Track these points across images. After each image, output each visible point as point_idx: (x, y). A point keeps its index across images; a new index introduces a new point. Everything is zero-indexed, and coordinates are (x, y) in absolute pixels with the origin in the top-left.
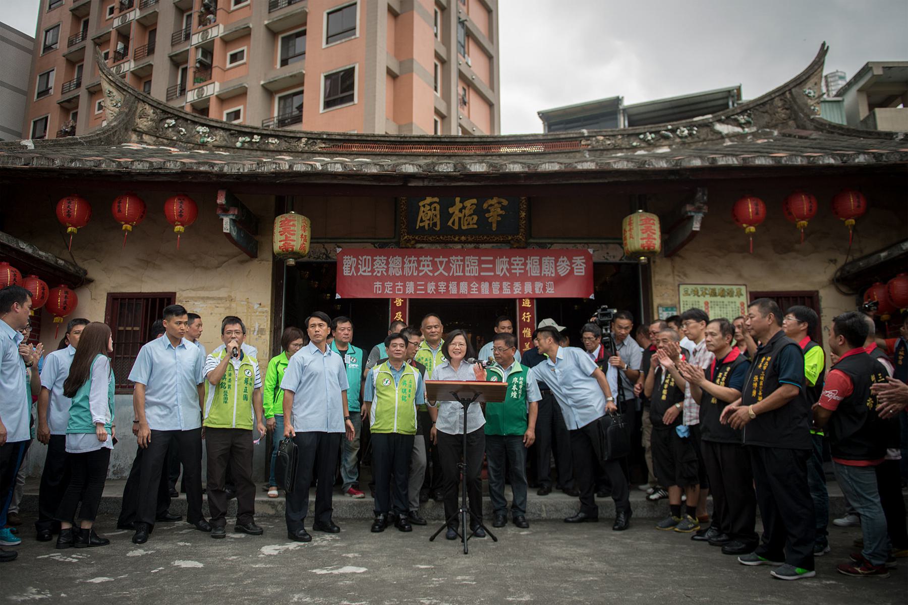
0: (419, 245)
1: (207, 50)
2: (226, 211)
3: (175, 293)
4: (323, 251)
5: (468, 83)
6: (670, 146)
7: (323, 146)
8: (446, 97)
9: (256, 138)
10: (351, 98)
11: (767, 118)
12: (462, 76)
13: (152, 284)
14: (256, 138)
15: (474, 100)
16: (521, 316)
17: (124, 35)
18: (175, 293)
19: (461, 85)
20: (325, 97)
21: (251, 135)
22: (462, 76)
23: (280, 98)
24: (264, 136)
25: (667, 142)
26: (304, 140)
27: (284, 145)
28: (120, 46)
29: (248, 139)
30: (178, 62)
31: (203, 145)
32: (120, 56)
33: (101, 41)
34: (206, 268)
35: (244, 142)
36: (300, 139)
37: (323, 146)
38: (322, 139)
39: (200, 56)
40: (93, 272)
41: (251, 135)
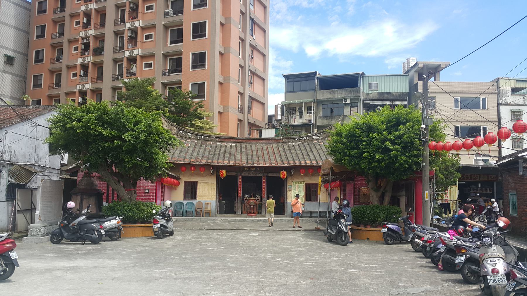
1: (134, 31)
5: (253, 48)
8: (244, 58)
9: (203, 137)
10: (204, 66)
11: (325, 135)
12: (251, 45)
13: (193, 179)
14: (203, 137)
15: (256, 55)
17: (87, 14)
19: (251, 49)
20: (192, 64)
21: (201, 136)
22: (251, 45)
23: (170, 59)
27: (209, 139)
28: (85, 20)
30: (118, 34)
31: (189, 138)
32: (86, 26)
33: (73, 16)
39: (130, 34)
41: (201, 136)
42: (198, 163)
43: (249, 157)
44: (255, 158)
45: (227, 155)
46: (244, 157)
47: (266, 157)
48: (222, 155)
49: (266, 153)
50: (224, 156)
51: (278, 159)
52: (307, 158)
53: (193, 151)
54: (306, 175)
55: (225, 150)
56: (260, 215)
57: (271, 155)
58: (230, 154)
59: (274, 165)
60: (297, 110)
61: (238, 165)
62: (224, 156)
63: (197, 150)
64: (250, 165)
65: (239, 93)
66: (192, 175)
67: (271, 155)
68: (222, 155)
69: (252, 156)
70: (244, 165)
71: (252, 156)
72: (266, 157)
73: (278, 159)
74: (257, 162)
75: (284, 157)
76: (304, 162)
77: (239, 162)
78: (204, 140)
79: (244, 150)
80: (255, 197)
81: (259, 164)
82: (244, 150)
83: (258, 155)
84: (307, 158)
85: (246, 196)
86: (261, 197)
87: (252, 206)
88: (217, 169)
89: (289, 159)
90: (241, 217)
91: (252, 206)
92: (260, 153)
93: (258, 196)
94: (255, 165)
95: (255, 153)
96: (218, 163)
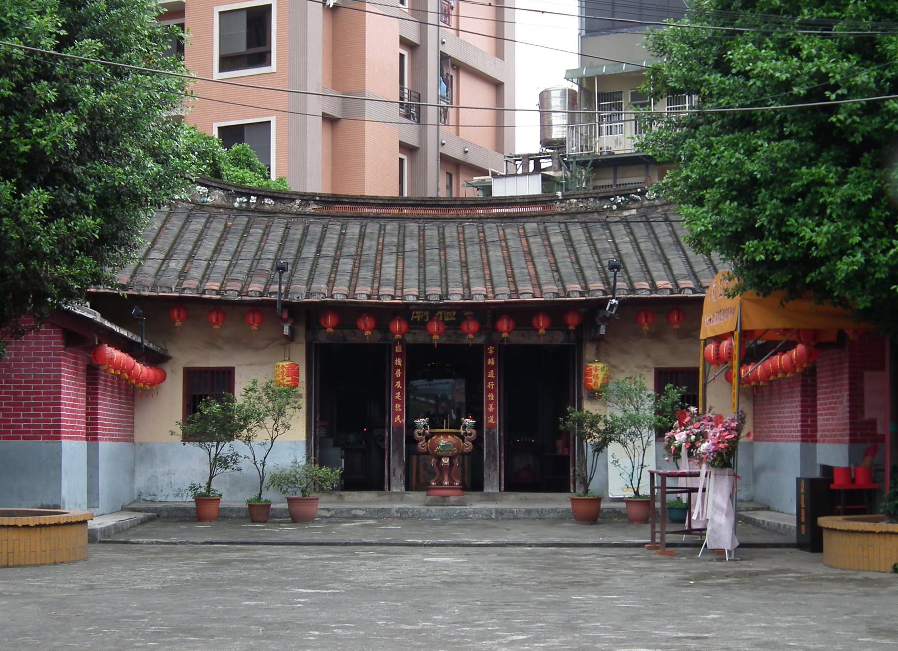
0: (412, 331)
2: (286, 321)
3: (234, 368)
4: (341, 335)
6: (637, 209)
7: (316, 207)
9: (253, 199)
13: (215, 361)
14: (253, 199)
16: (487, 385)
18: (234, 368)
21: (248, 196)
24: (260, 198)
25: (636, 205)
26: (298, 202)
29: (246, 200)
34: (257, 349)
35: (241, 203)
36: (294, 200)
37: (316, 207)
38: (315, 201)
40: (172, 352)
41: (248, 196)
42: (232, 296)
43: (433, 269)
44: (454, 274)
45: (346, 265)
46: (412, 273)
47: (499, 269)
48: (325, 265)
49: (496, 254)
50: (335, 266)
51: (545, 275)
52: (657, 269)
53: (217, 250)
54: (656, 336)
55: (339, 247)
56: (476, 495)
57: (519, 262)
58: (358, 258)
59: (528, 298)
60: (626, 100)
61: (388, 300)
62: (335, 266)
63: (231, 246)
64: (434, 299)
65: (404, 42)
66: (212, 344)
67: (519, 262)
68: (325, 265)
69: (444, 268)
70: (411, 299)
71: (444, 268)
72: (499, 269)
73: (545, 275)
74: (460, 290)
75: (567, 268)
76: (646, 285)
77: (390, 290)
78: (259, 211)
79: (412, 244)
80: (457, 424)
81: (471, 296)
82: (412, 244)
83: (465, 265)
84: (657, 269)
85: (421, 421)
86: (478, 426)
87: (445, 461)
88: (307, 315)
89: (588, 273)
90: (402, 500)
91: (445, 461)
92: (474, 254)
93: (469, 421)
94: (456, 299)
95: (453, 254)
96: (309, 294)
